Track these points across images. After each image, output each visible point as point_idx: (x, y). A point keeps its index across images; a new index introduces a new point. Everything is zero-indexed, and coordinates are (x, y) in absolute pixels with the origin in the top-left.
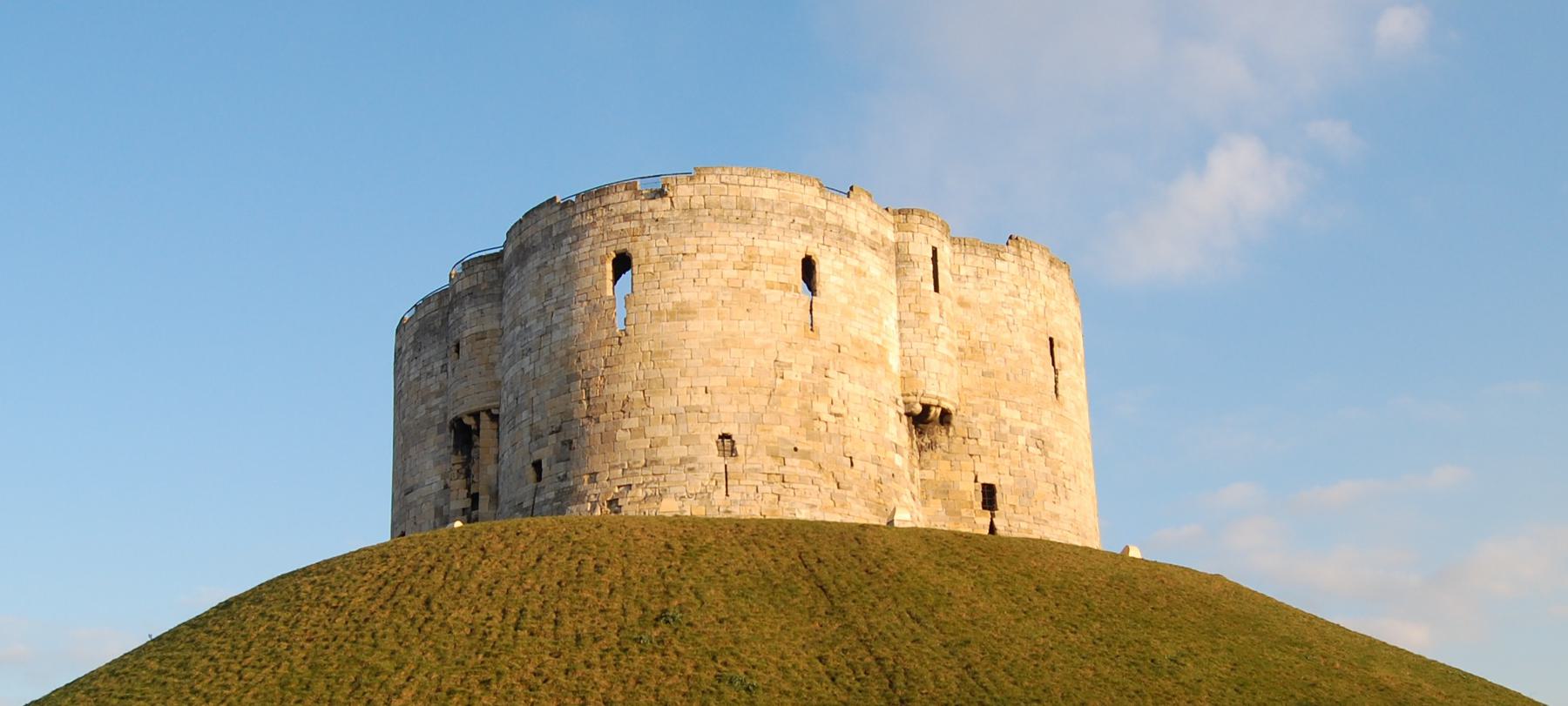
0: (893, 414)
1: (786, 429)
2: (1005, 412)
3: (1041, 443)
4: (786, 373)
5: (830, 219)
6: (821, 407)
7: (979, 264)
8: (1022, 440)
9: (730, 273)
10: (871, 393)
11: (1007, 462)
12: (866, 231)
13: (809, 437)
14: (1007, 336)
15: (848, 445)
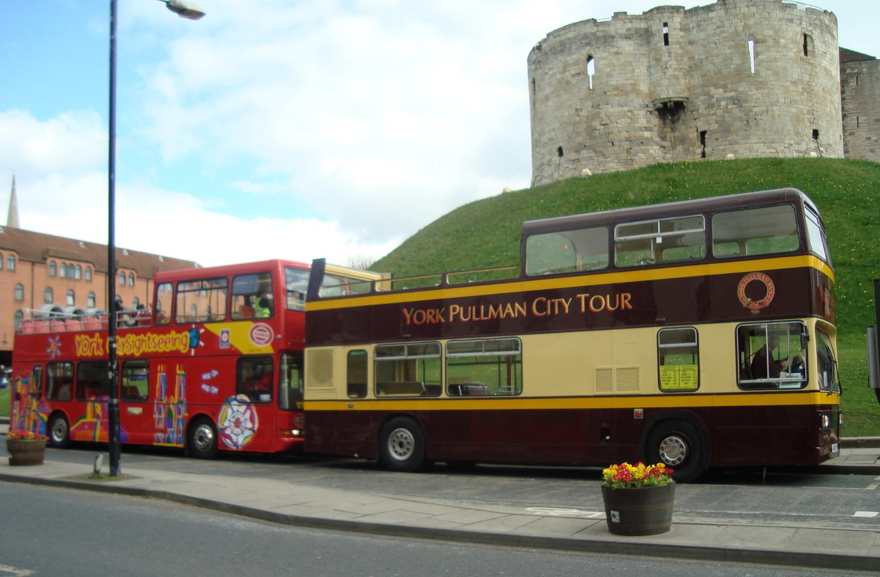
0: (642, 113)
1: (580, 138)
2: (713, 90)
3: (737, 101)
4: (580, 113)
5: (599, 34)
6: (596, 124)
7: (699, 18)
8: (723, 103)
9: (559, 76)
10: (626, 109)
11: (714, 117)
12: (623, 31)
13: (591, 139)
14: (716, 51)
15: (611, 136)
